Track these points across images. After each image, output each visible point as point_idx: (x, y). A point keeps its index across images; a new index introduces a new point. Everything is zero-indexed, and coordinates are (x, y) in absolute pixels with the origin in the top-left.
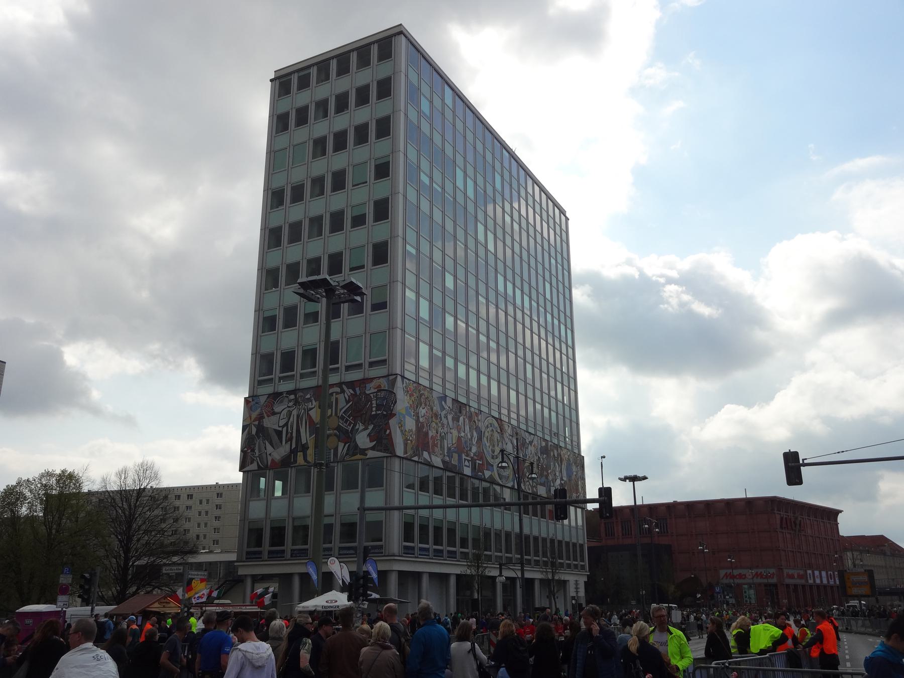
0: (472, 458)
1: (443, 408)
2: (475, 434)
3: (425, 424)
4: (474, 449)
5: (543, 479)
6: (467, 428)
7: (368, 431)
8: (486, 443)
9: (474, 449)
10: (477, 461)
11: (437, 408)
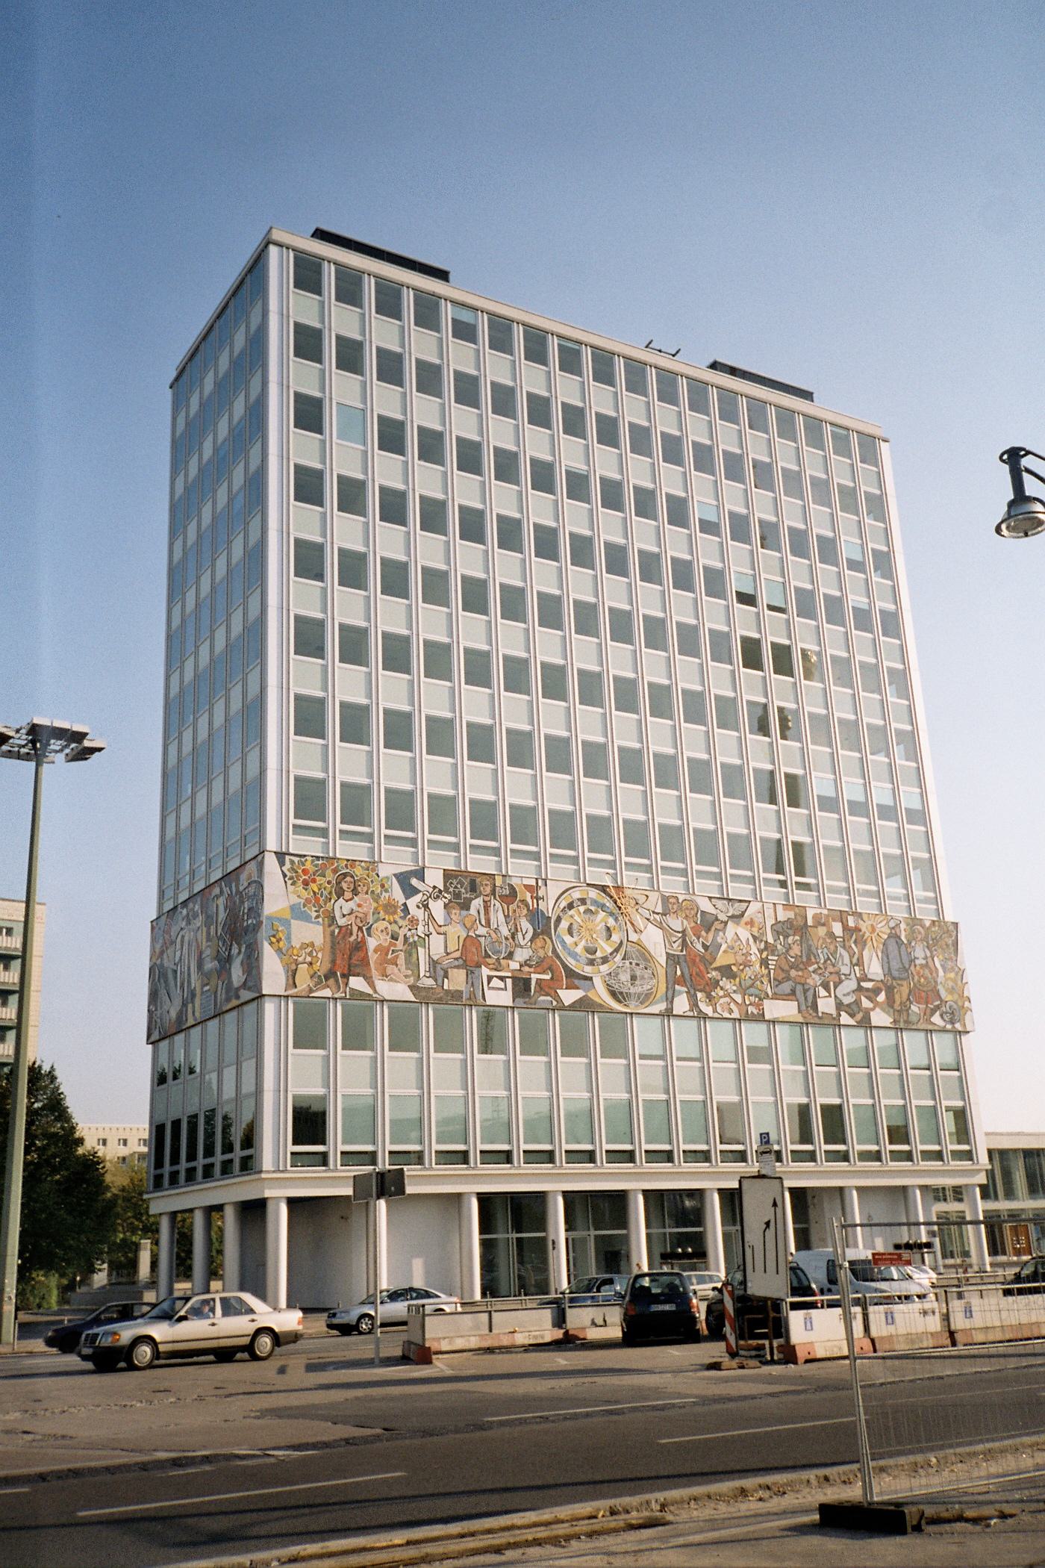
0: (513, 971)
2: (525, 925)
3: (355, 929)
4: (521, 955)
5: (786, 987)
6: (498, 917)
7: (241, 956)
8: (568, 939)
9: (521, 955)
10: (534, 977)
11: (397, 894)
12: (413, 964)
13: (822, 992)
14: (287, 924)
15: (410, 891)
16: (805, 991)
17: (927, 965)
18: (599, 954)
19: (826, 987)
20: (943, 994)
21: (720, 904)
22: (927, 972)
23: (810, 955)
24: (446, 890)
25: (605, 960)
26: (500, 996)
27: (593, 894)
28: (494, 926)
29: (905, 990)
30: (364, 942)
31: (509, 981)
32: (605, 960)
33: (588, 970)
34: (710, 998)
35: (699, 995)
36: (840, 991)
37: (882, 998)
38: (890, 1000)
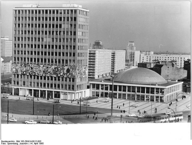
1: (21, 66)
2: (31, 69)
5: (55, 73)
6: (28, 68)
8: (34, 70)
9: (30, 71)
14: (13, 69)
15: (21, 66)
18: (37, 71)
19: (59, 73)
20: (73, 74)
23: (58, 70)
26: (28, 74)
29: (68, 74)
32: (37, 71)
36: (61, 74)
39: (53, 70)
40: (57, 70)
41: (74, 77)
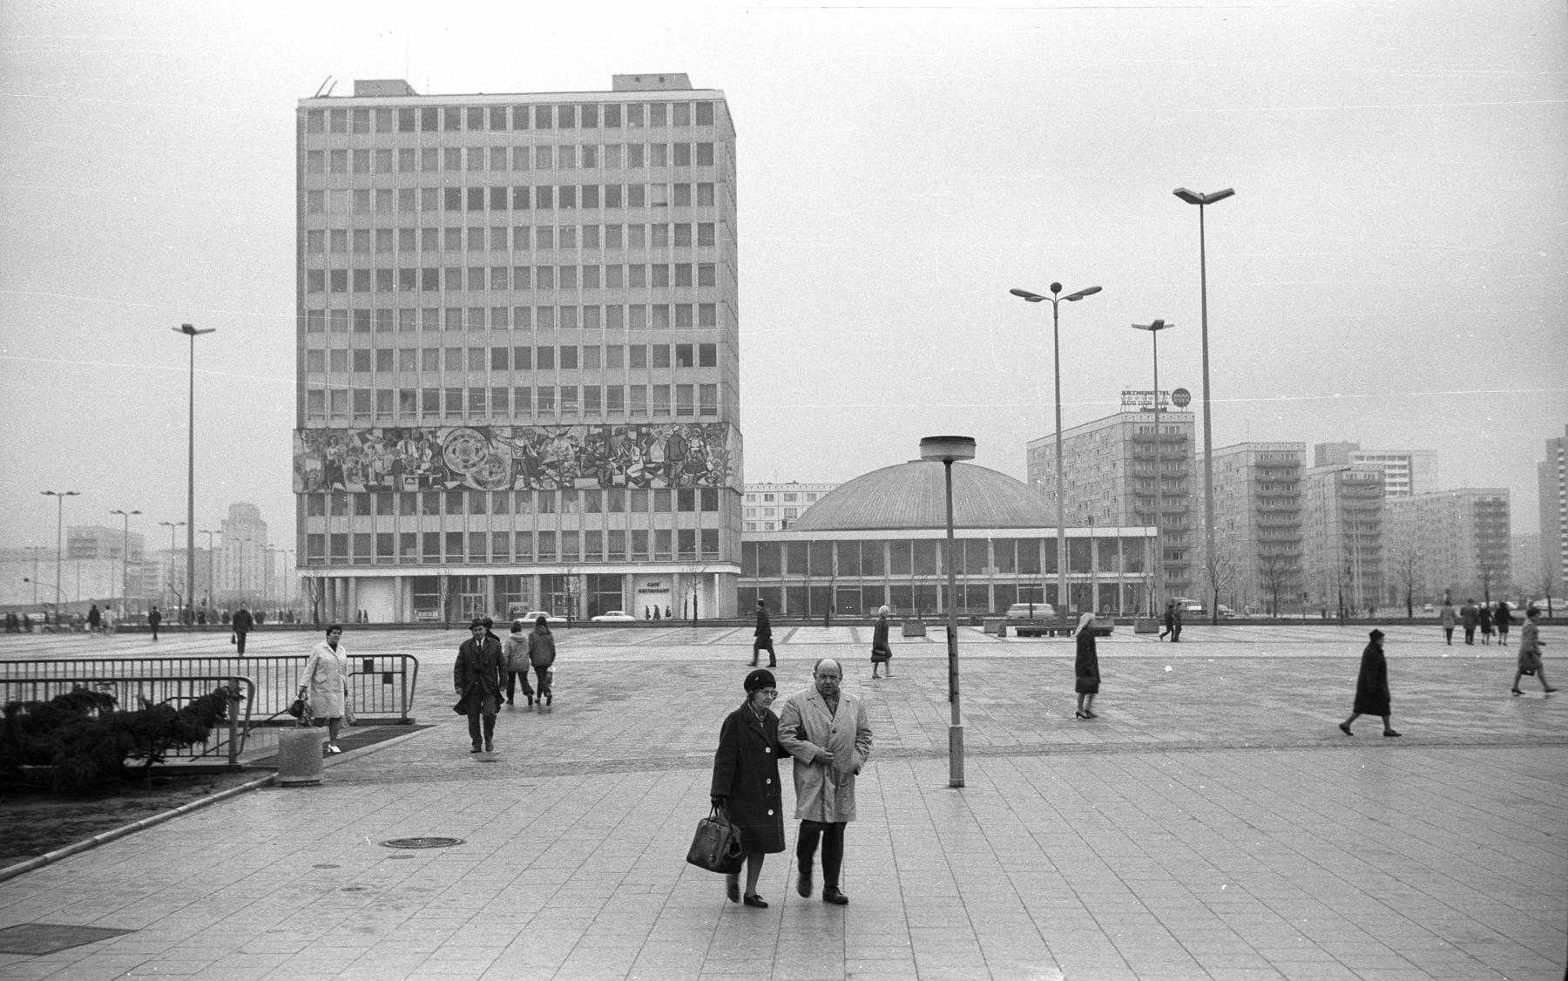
2: (428, 452)
5: (592, 470)
6: (413, 449)
9: (425, 466)
11: (357, 442)
12: (366, 476)
13: (617, 472)
15: (364, 440)
16: (605, 472)
17: (700, 451)
18: (471, 462)
19: (620, 468)
20: (710, 466)
21: (550, 429)
22: (699, 455)
23: (612, 451)
24: (384, 437)
25: (474, 465)
26: (412, 487)
27: (468, 431)
28: (410, 453)
29: (680, 466)
30: (341, 466)
31: (417, 480)
32: (474, 465)
33: (463, 471)
34: (538, 479)
35: (532, 479)
36: (629, 471)
37: (662, 471)
38: (667, 474)
39: (582, 450)
40: (602, 450)
41: (715, 482)
